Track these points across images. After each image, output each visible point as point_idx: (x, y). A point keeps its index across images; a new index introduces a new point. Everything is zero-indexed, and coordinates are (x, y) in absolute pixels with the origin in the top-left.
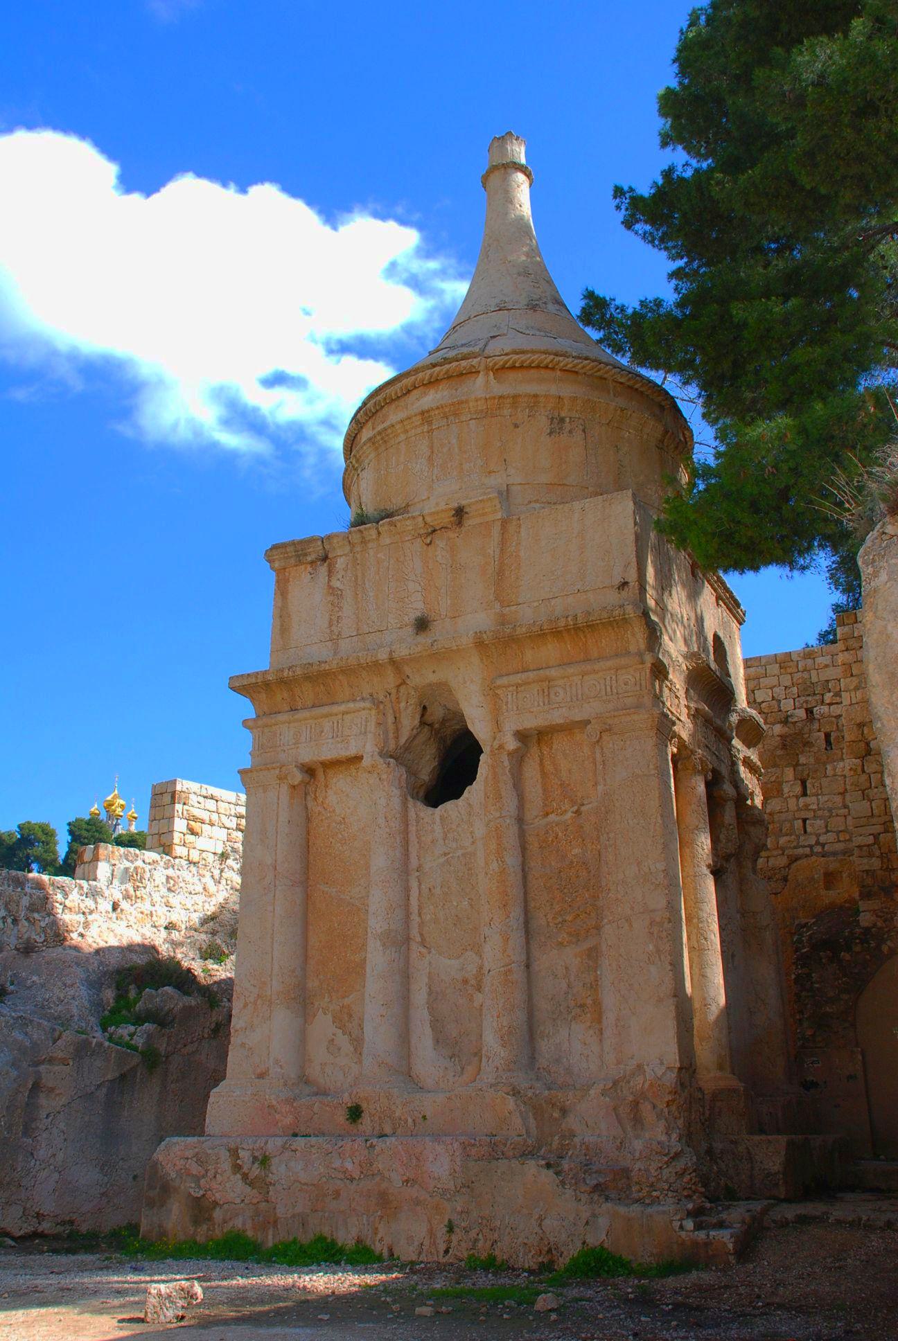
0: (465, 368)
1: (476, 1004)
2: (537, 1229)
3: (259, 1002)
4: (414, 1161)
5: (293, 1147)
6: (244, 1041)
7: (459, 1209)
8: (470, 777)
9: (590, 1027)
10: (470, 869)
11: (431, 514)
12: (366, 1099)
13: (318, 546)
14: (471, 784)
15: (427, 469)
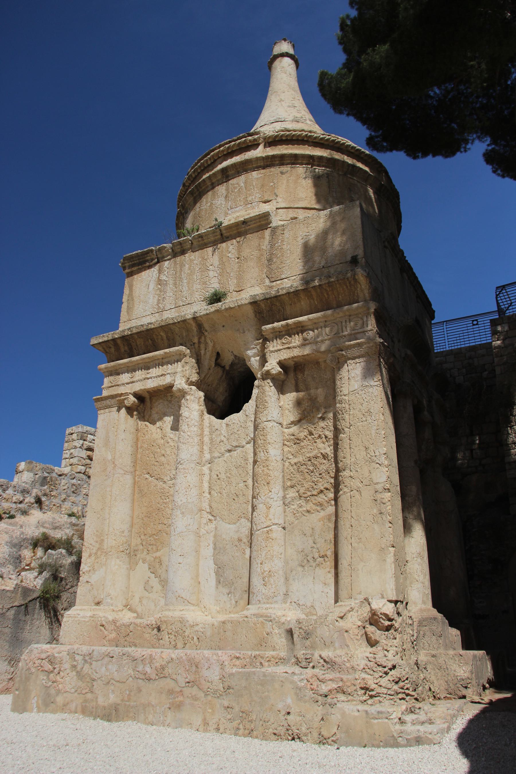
0: (250, 141)
3: (99, 553)
4: (194, 668)
5: (111, 655)
7: (226, 704)
8: (247, 398)
12: (165, 622)
14: (248, 402)
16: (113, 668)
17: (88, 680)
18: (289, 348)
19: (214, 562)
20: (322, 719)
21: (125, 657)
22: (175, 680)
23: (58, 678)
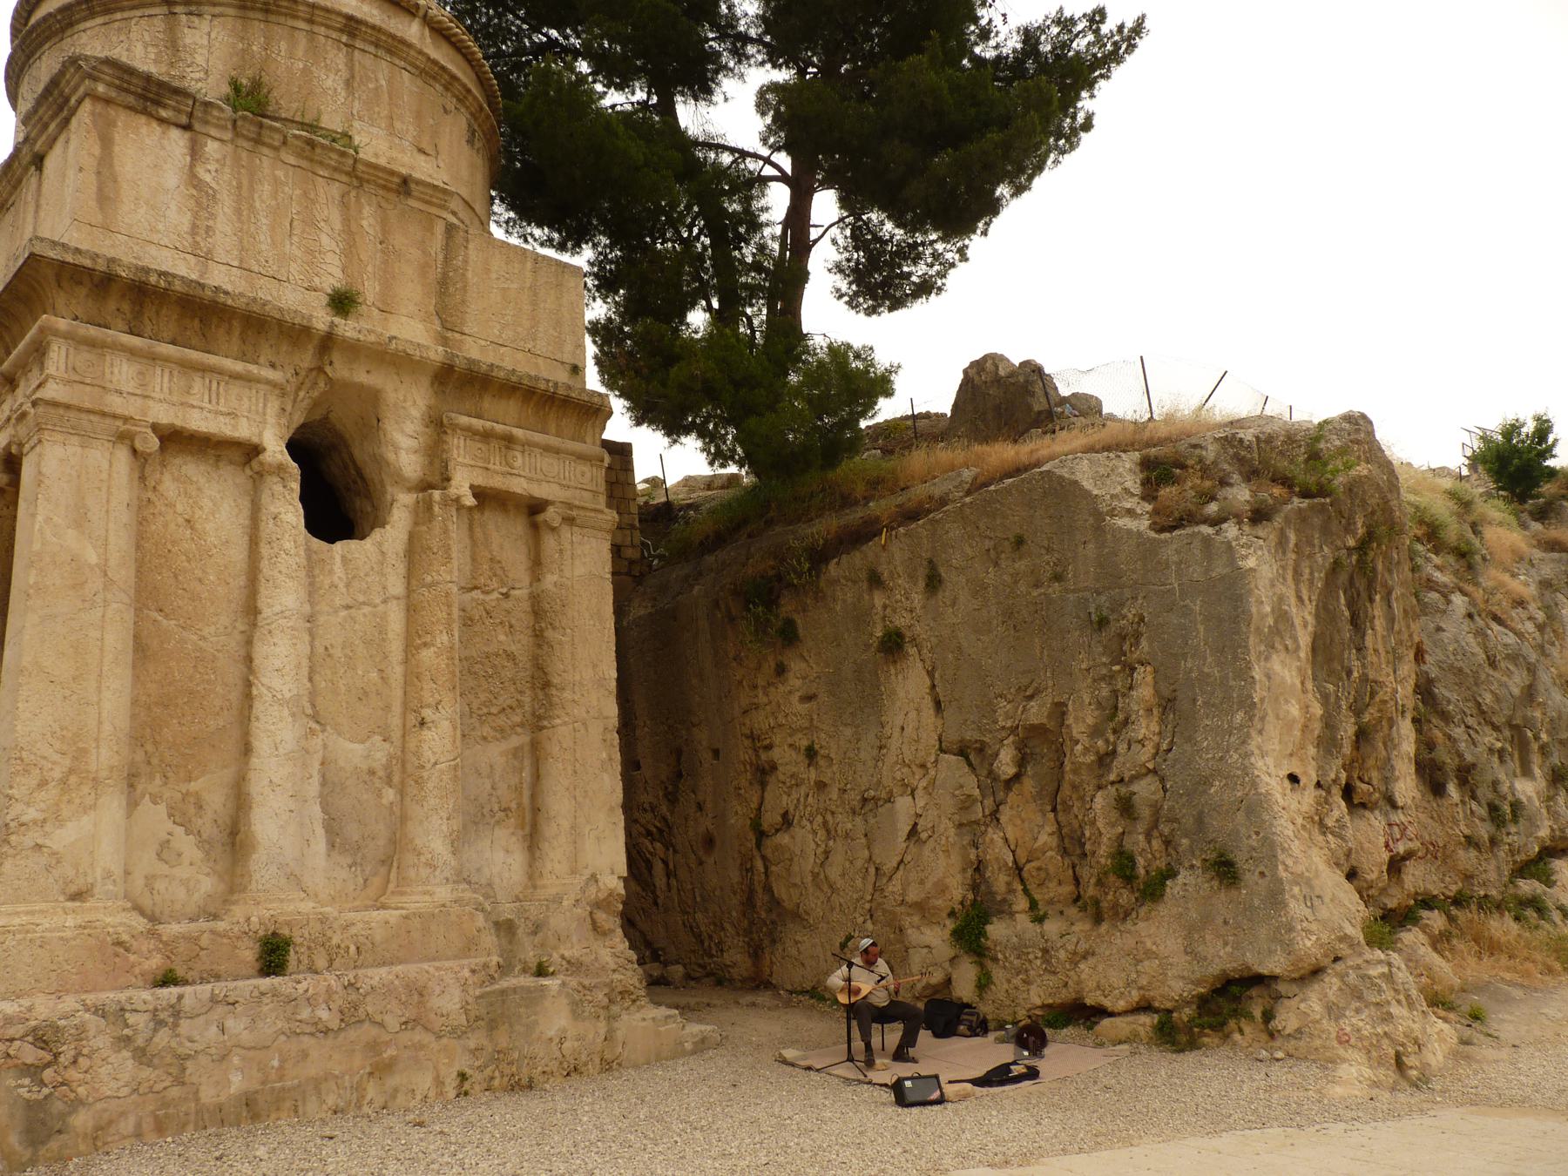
1: (384, 801)
2: (558, 1054)
3: (73, 779)
4: (416, 997)
5: (231, 1001)
6: (39, 841)
7: (472, 1044)
9: (513, 834)
10: (380, 633)
11: (369, 165)
13: (187, 105)
15: (343, 94)
16: (236, 1025)
17: (168, 1059)
18: (487, 469)
19: (322, 808)
20: (606, 1039)
21: (265, 1000)
22: (381, 1025)
23: (73, 1074)
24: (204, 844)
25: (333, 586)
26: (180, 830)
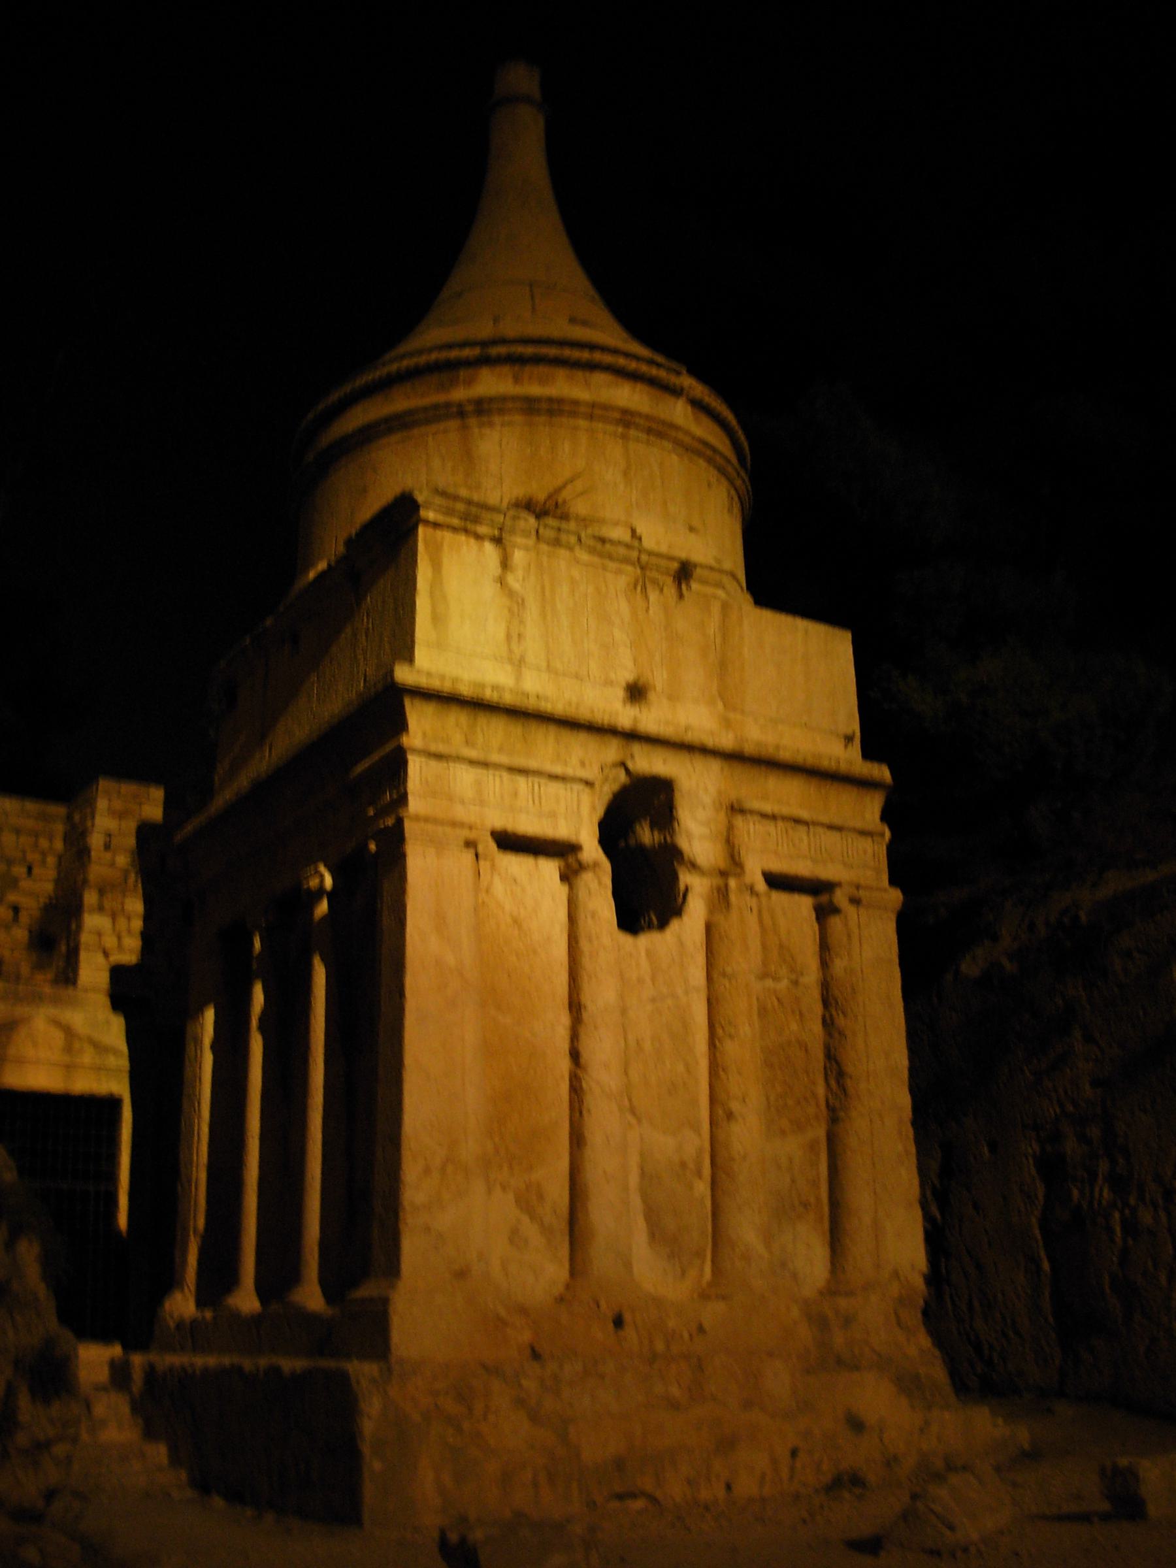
3: (450, 1168)
11: (650, 553)
24: (546, 1231)
25: (640, 981)
26: (525, 1219)
